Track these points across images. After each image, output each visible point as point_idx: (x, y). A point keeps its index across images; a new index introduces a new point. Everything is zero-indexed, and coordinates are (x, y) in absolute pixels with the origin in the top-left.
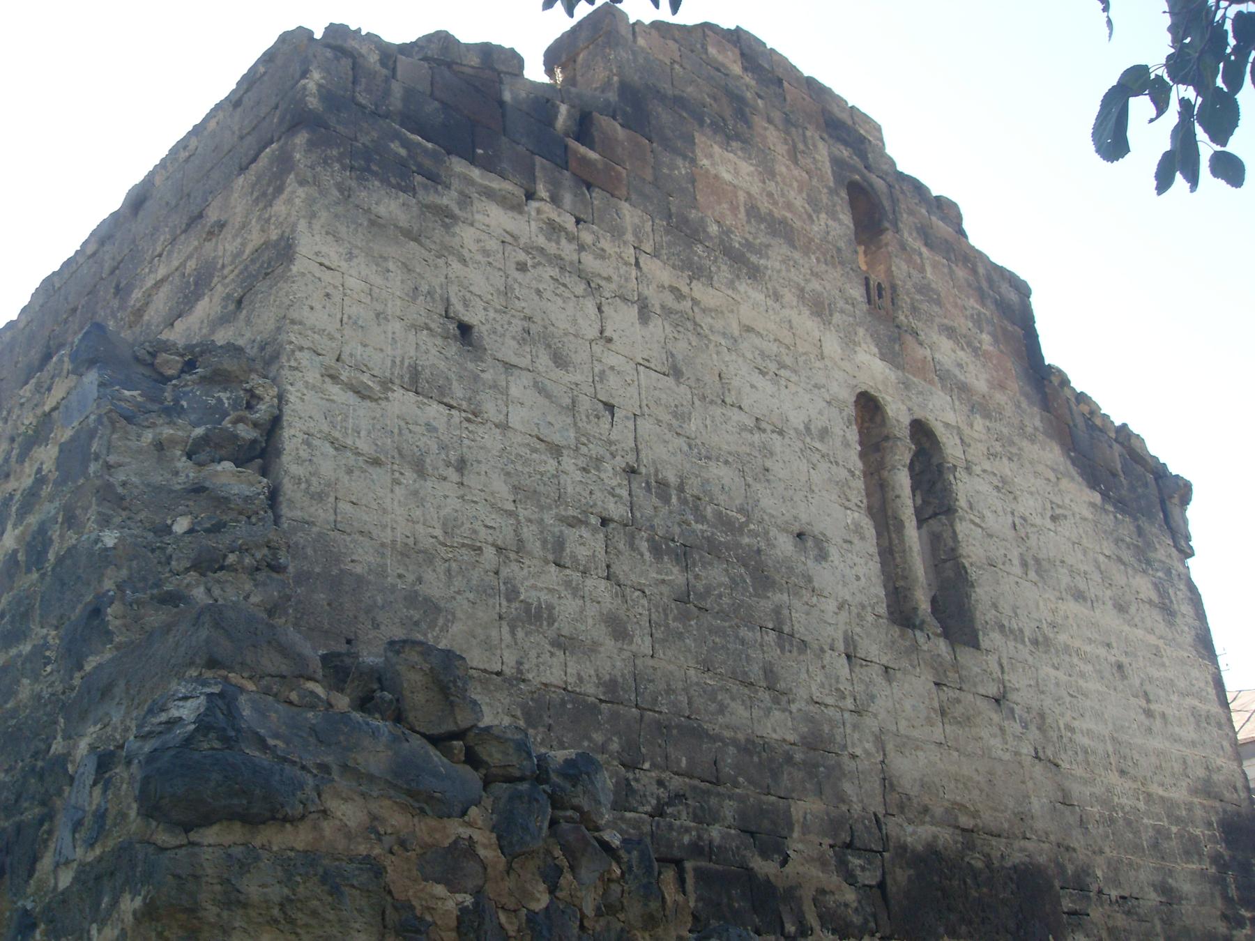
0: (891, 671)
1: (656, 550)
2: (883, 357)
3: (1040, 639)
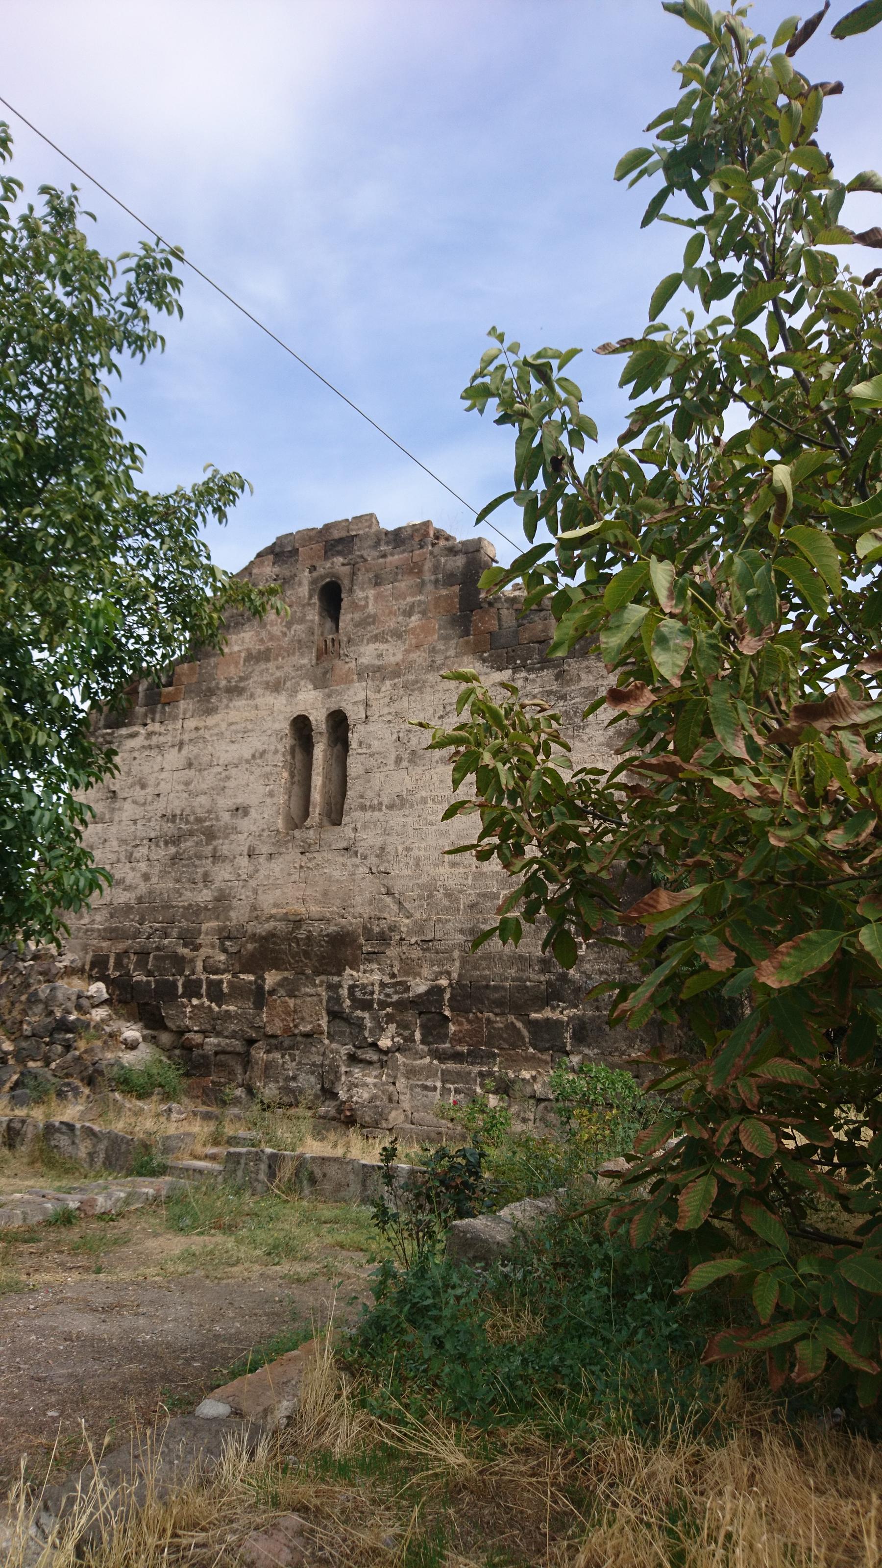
1: (166, 843)
2: (316, 688)
3: (397, 801)
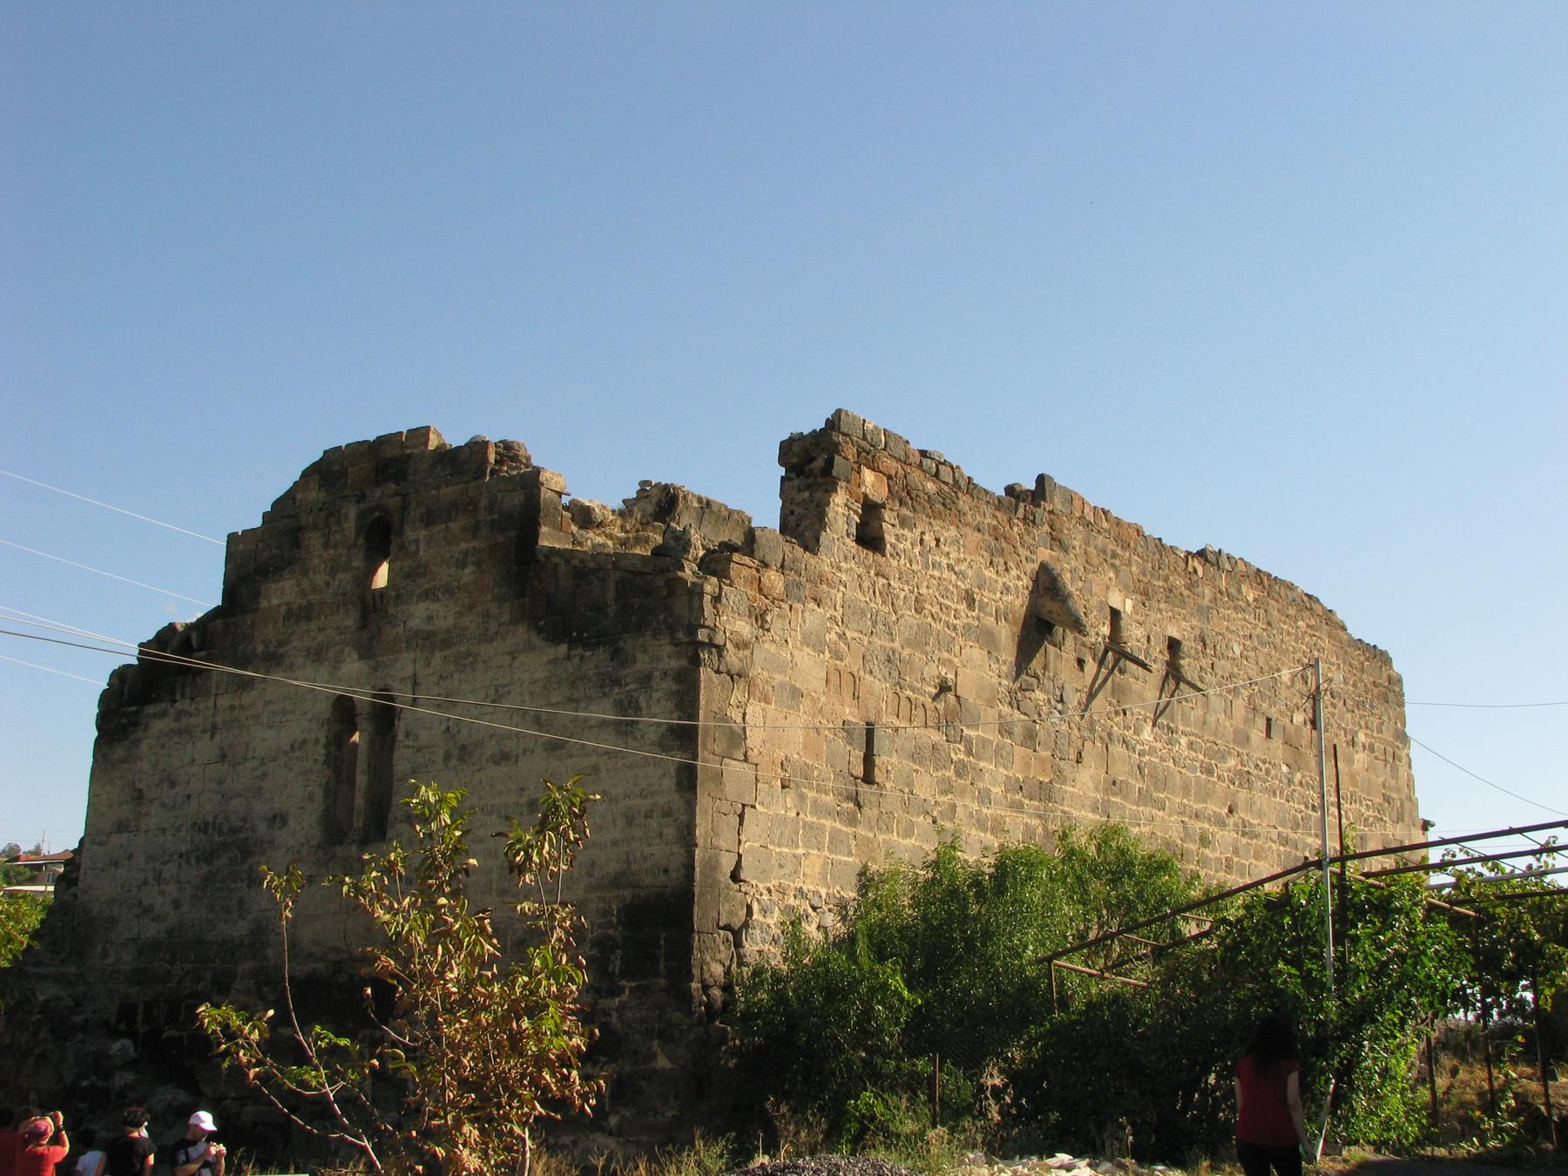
1: (198, 860)
2: (361, 658)
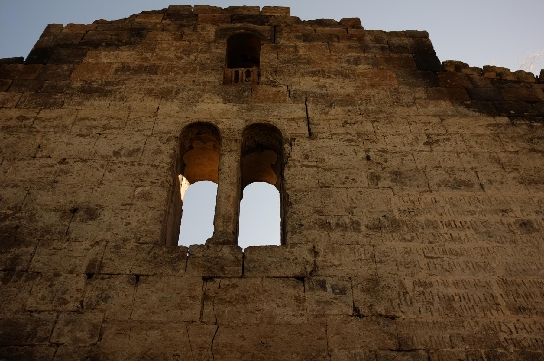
0: (141, 278)
2: (226, 101)
3: (385, 222)
